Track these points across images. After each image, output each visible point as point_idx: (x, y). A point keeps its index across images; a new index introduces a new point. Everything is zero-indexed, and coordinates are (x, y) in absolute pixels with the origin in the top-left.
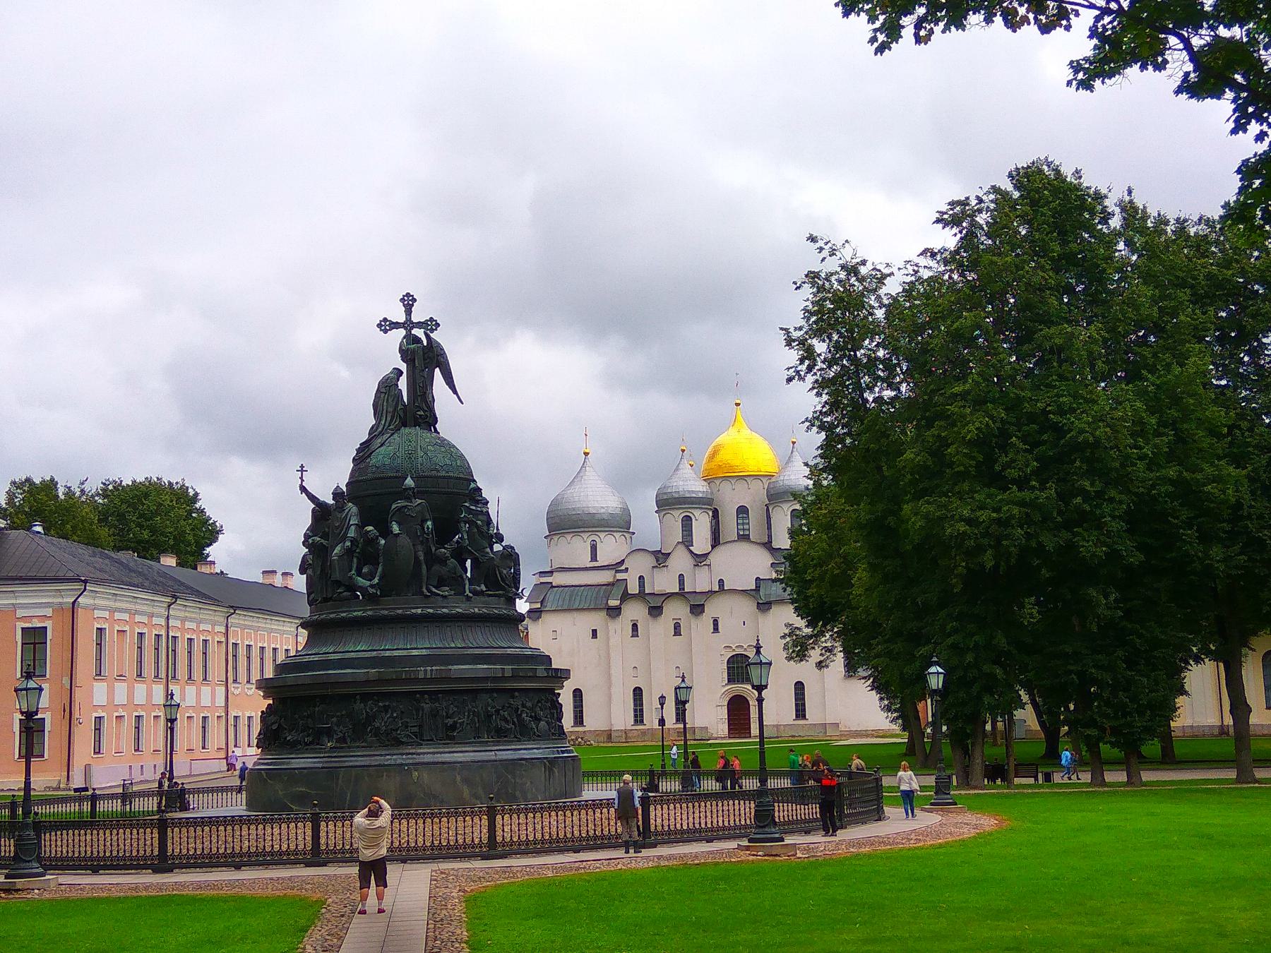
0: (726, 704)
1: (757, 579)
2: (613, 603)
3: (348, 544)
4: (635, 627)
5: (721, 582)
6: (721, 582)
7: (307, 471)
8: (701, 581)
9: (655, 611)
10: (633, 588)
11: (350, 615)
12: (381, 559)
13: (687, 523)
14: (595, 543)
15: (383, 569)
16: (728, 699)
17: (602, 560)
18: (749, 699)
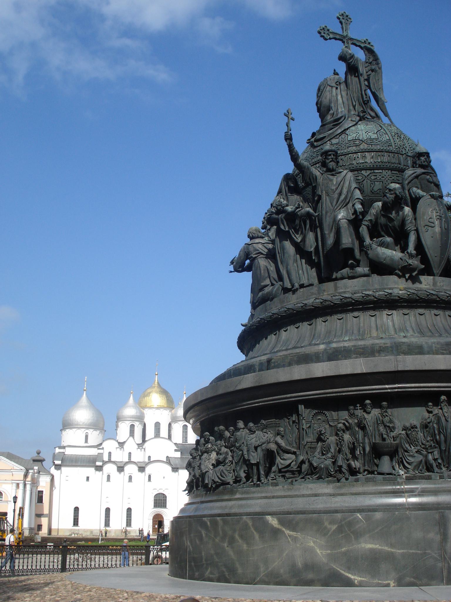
0: (152, 518)
1: (167, 457)
2: (99, 464)
3: (359, 207)
4: (109, 477)
5: (149, 457)
6: (149, 457)
7: (293, 119)
8: (139, 456)
9: (121, 469)
10: (106, 458)
11: (381, 293)
12: (410, 227)
13: (132, 426)
14: (87, 434)
15: (419, 239)
16: (153, 516)
17: (90, 443)
18: (163, 516)
